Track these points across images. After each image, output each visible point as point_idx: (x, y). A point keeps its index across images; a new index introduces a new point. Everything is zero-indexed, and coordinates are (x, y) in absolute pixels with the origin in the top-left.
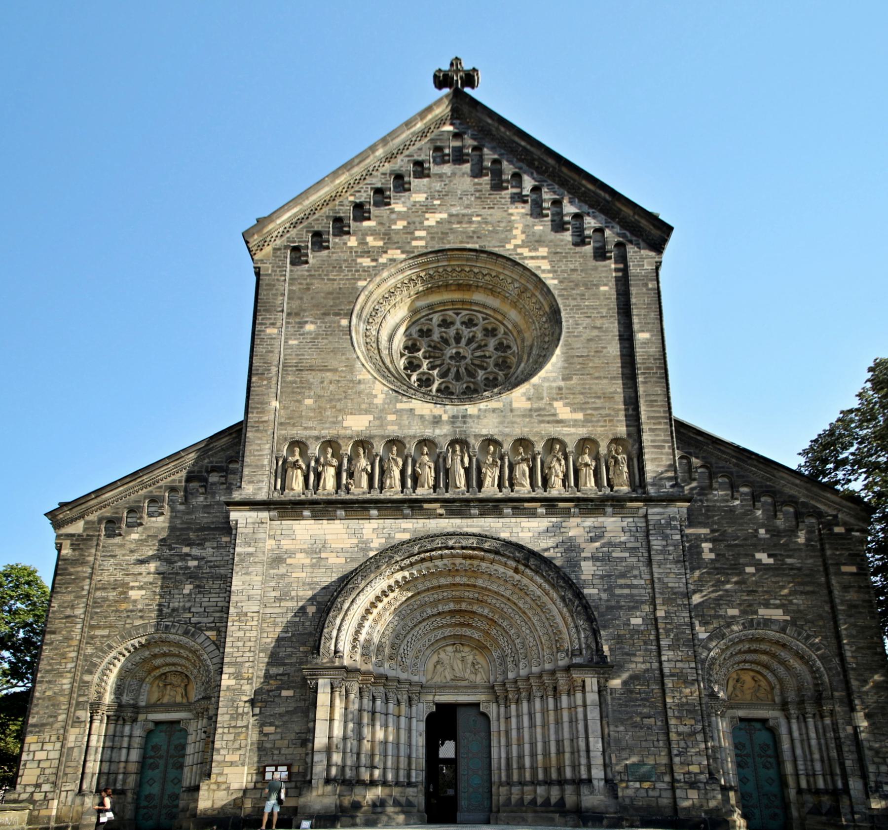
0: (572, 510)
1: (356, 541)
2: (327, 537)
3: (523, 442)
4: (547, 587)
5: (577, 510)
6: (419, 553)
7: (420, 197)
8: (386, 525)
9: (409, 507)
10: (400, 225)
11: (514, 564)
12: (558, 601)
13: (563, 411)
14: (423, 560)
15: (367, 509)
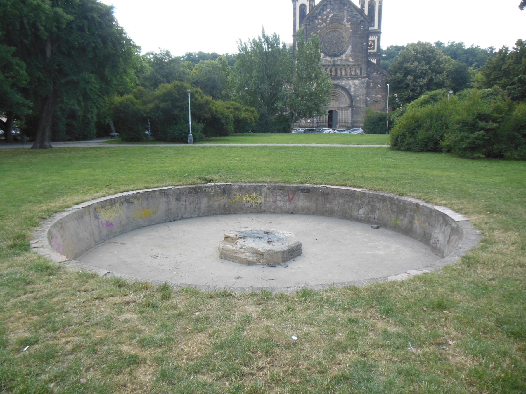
3: (344, 65)
7: (328, 10)
10: (325, 17)
13: (351, 60)
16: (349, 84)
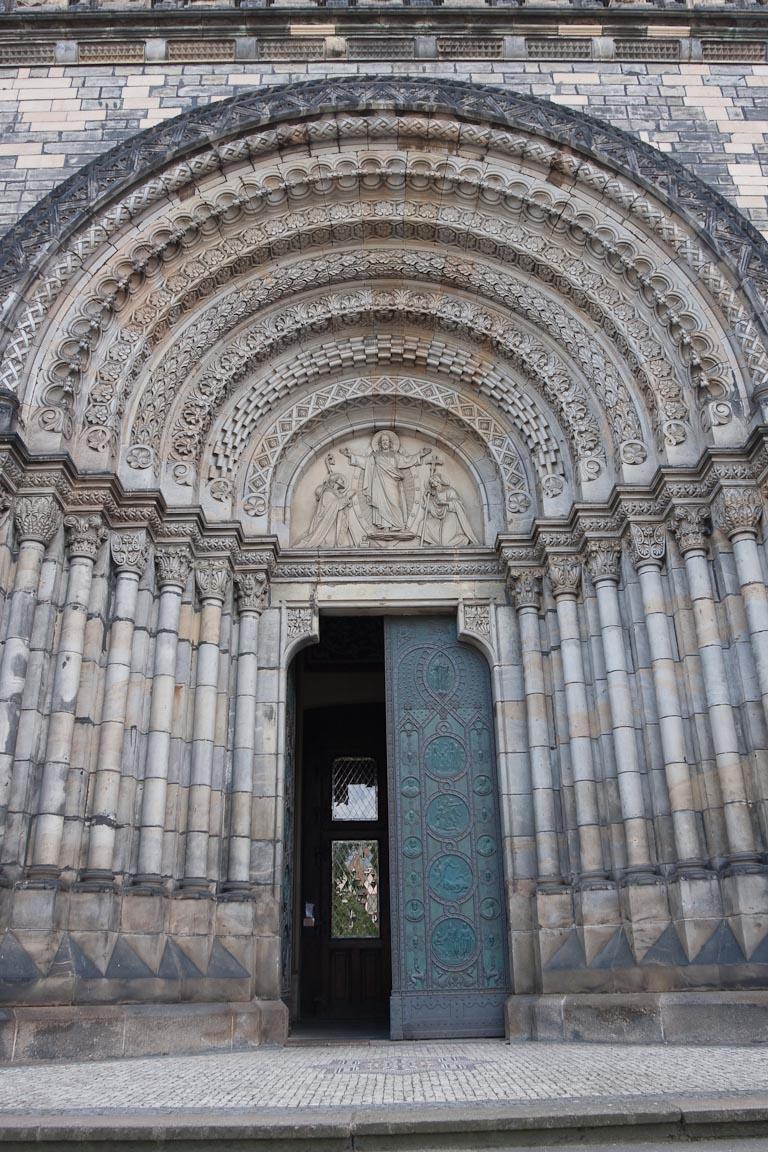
0: (685, 43)
1: (101, 115)
2: (23, 107)
4: (652, 209)
5: (697, 47)
6: (272, 125)
8: (186, 80)
9: (252, 32)
11: (548, 152)
12: (691, 248)
14: (284, 146)
15: (138, 40)
16: (676, 102)
